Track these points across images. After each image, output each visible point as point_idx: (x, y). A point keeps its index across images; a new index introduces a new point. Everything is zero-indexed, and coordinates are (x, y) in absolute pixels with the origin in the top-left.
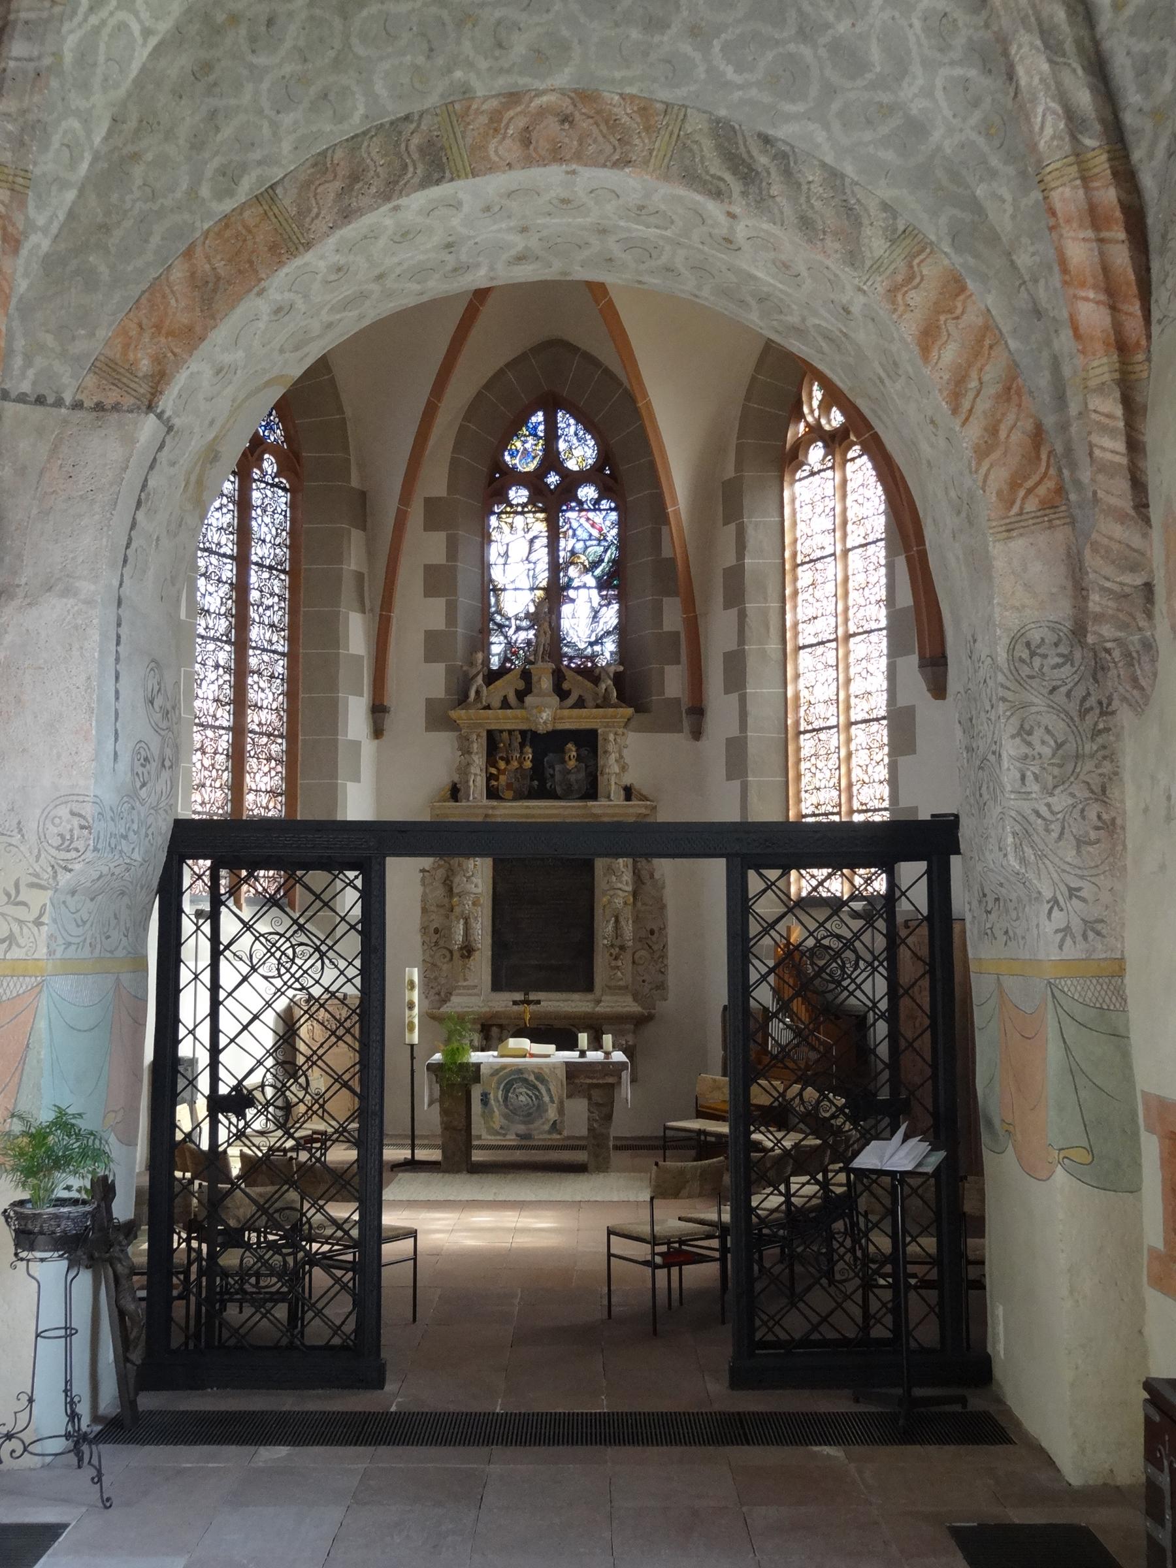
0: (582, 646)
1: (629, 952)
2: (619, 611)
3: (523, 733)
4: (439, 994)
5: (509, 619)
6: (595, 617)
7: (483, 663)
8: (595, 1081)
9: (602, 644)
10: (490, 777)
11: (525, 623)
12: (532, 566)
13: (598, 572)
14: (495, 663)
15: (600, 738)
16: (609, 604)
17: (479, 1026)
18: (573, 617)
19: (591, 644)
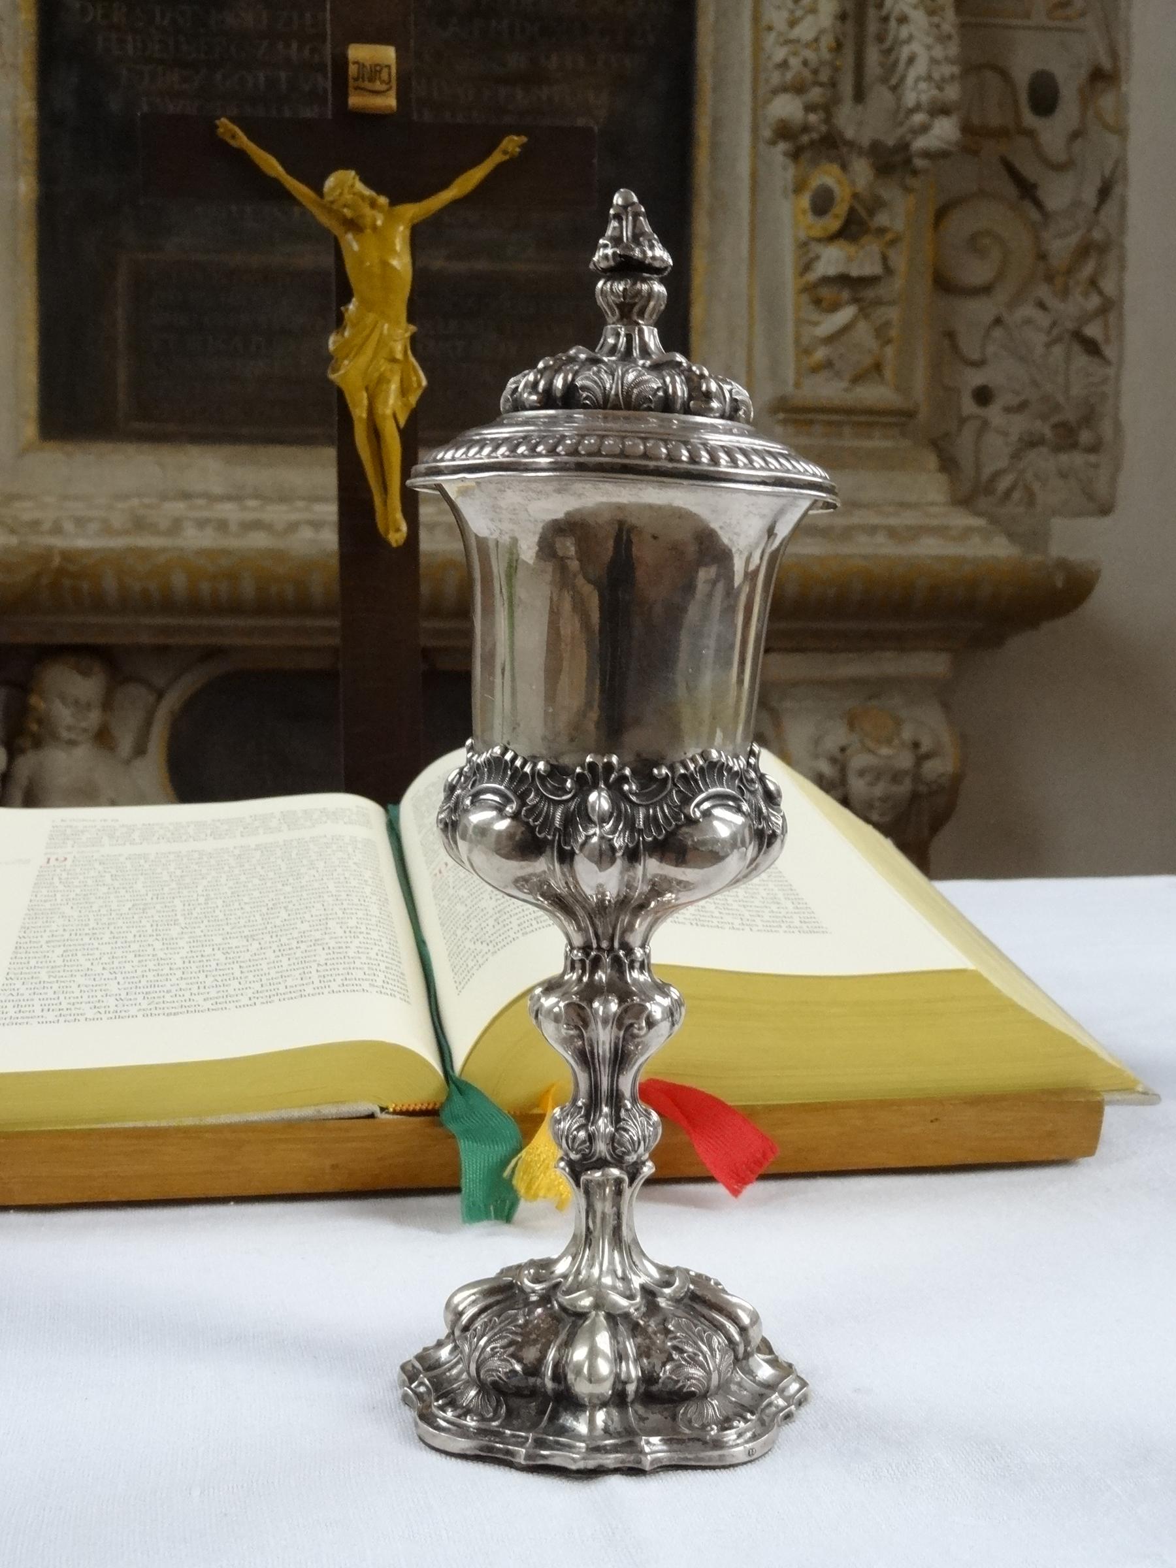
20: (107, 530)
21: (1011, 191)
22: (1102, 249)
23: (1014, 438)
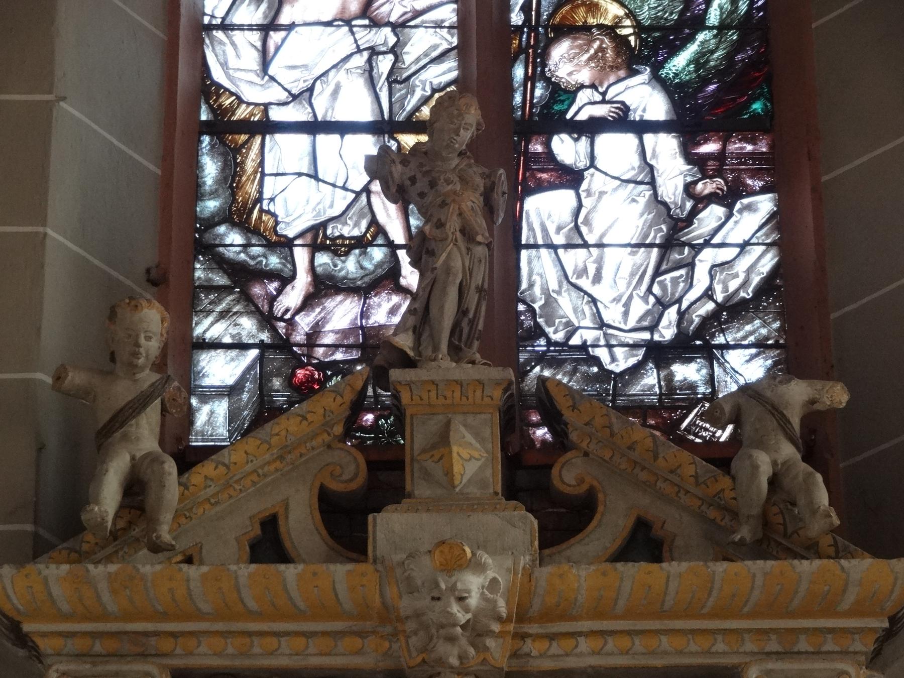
5: (285, 245)
6: (668, 245)
7: (160, 365)
11: (350, 266)
12: (386, 36)
13: (680, 62)
18: (577, 242)
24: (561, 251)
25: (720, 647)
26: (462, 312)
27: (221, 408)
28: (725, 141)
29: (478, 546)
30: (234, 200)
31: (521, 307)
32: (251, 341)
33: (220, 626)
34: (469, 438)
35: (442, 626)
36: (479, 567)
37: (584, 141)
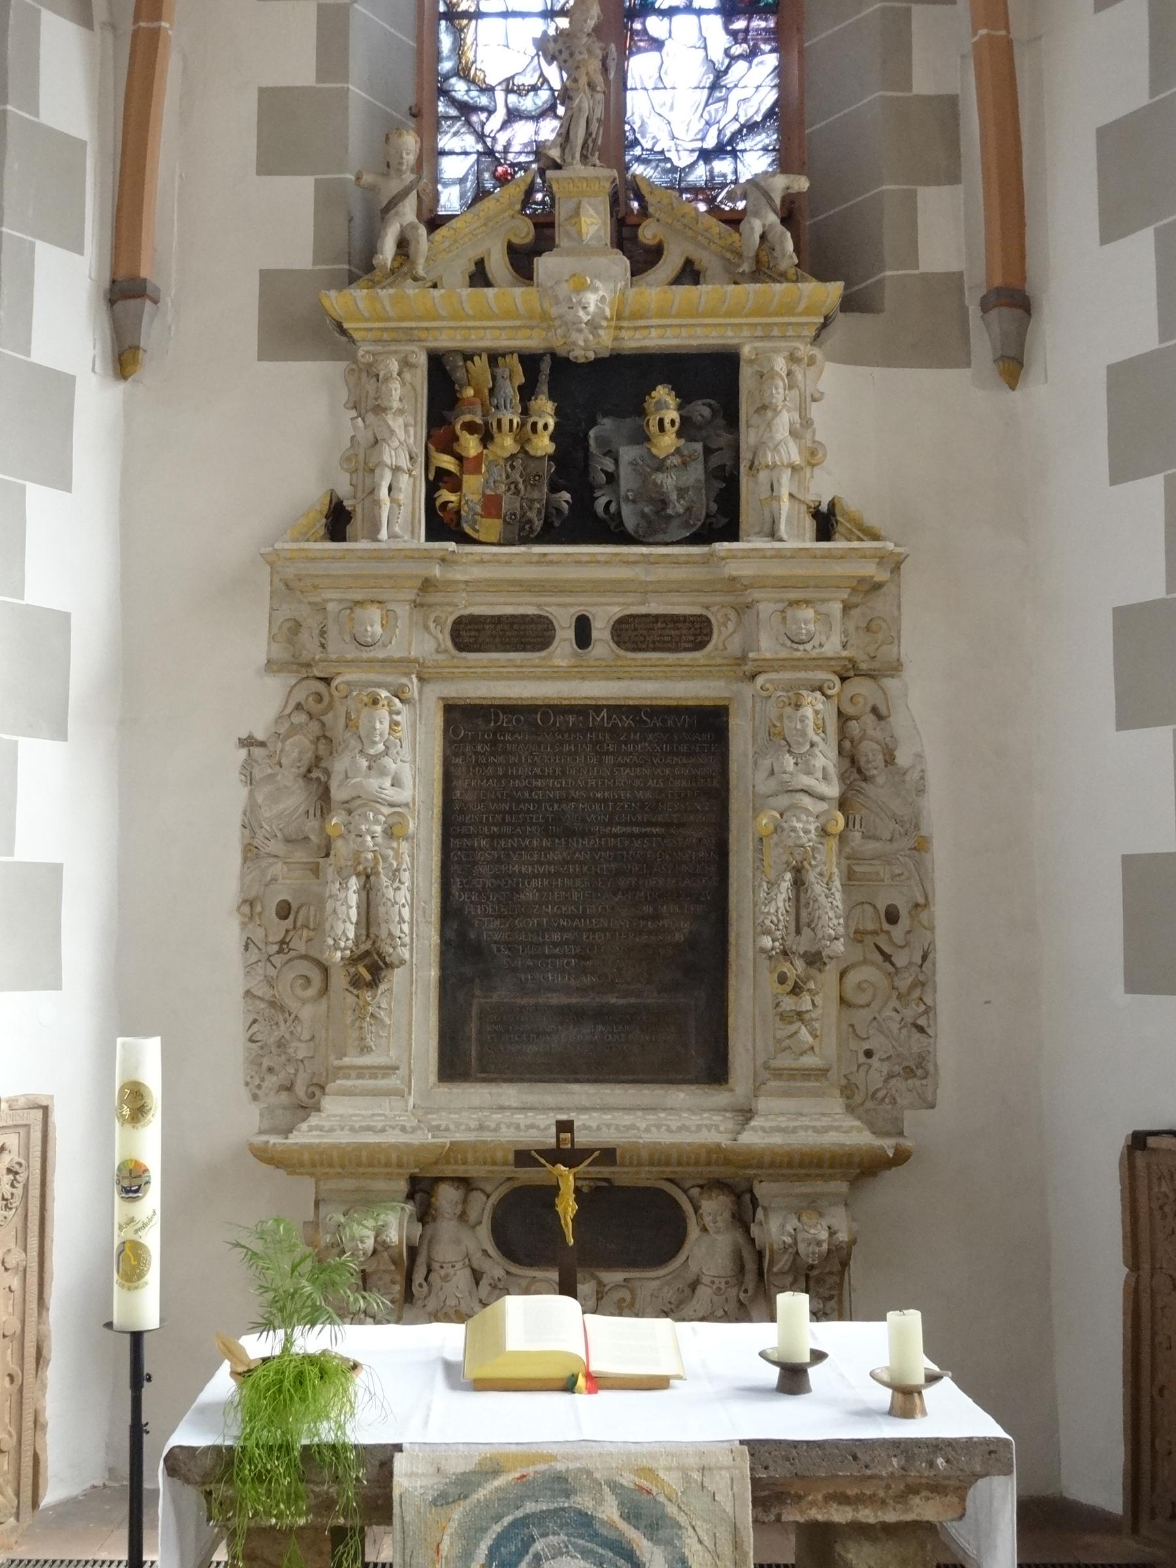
0: (683, 160)
1: (831, 973)
2: (781, 71)
3: (530, 361)
4: (289, 1088)
5: (490, 90)
6: (714, 87)
8: (867, 1515)
9: (734, 154)
10: (438, 480)
11: (528, 103)
14: (450, 200)
15: (746, 375)
16: (750, 56)
17: (403, 1186)
19: (706, 155)
20: (469, 1129)
21: (878, 958)
22: (923, 984)
23: (885, 1073)
24: (650, 92)
25: (730, 333)
26: (588, 134)
27: (455, 191)
28: (750, 20)
29: (597, 276)
30: (460, 62)
31: (627, 127)
32: (471, 150)
33: (452, 324)
34: (592, 212)
35: (574, 324)
36: (595, 290)
37: (666, 20)
